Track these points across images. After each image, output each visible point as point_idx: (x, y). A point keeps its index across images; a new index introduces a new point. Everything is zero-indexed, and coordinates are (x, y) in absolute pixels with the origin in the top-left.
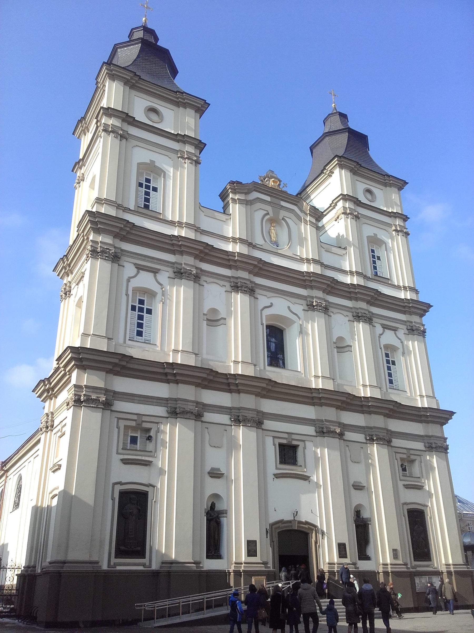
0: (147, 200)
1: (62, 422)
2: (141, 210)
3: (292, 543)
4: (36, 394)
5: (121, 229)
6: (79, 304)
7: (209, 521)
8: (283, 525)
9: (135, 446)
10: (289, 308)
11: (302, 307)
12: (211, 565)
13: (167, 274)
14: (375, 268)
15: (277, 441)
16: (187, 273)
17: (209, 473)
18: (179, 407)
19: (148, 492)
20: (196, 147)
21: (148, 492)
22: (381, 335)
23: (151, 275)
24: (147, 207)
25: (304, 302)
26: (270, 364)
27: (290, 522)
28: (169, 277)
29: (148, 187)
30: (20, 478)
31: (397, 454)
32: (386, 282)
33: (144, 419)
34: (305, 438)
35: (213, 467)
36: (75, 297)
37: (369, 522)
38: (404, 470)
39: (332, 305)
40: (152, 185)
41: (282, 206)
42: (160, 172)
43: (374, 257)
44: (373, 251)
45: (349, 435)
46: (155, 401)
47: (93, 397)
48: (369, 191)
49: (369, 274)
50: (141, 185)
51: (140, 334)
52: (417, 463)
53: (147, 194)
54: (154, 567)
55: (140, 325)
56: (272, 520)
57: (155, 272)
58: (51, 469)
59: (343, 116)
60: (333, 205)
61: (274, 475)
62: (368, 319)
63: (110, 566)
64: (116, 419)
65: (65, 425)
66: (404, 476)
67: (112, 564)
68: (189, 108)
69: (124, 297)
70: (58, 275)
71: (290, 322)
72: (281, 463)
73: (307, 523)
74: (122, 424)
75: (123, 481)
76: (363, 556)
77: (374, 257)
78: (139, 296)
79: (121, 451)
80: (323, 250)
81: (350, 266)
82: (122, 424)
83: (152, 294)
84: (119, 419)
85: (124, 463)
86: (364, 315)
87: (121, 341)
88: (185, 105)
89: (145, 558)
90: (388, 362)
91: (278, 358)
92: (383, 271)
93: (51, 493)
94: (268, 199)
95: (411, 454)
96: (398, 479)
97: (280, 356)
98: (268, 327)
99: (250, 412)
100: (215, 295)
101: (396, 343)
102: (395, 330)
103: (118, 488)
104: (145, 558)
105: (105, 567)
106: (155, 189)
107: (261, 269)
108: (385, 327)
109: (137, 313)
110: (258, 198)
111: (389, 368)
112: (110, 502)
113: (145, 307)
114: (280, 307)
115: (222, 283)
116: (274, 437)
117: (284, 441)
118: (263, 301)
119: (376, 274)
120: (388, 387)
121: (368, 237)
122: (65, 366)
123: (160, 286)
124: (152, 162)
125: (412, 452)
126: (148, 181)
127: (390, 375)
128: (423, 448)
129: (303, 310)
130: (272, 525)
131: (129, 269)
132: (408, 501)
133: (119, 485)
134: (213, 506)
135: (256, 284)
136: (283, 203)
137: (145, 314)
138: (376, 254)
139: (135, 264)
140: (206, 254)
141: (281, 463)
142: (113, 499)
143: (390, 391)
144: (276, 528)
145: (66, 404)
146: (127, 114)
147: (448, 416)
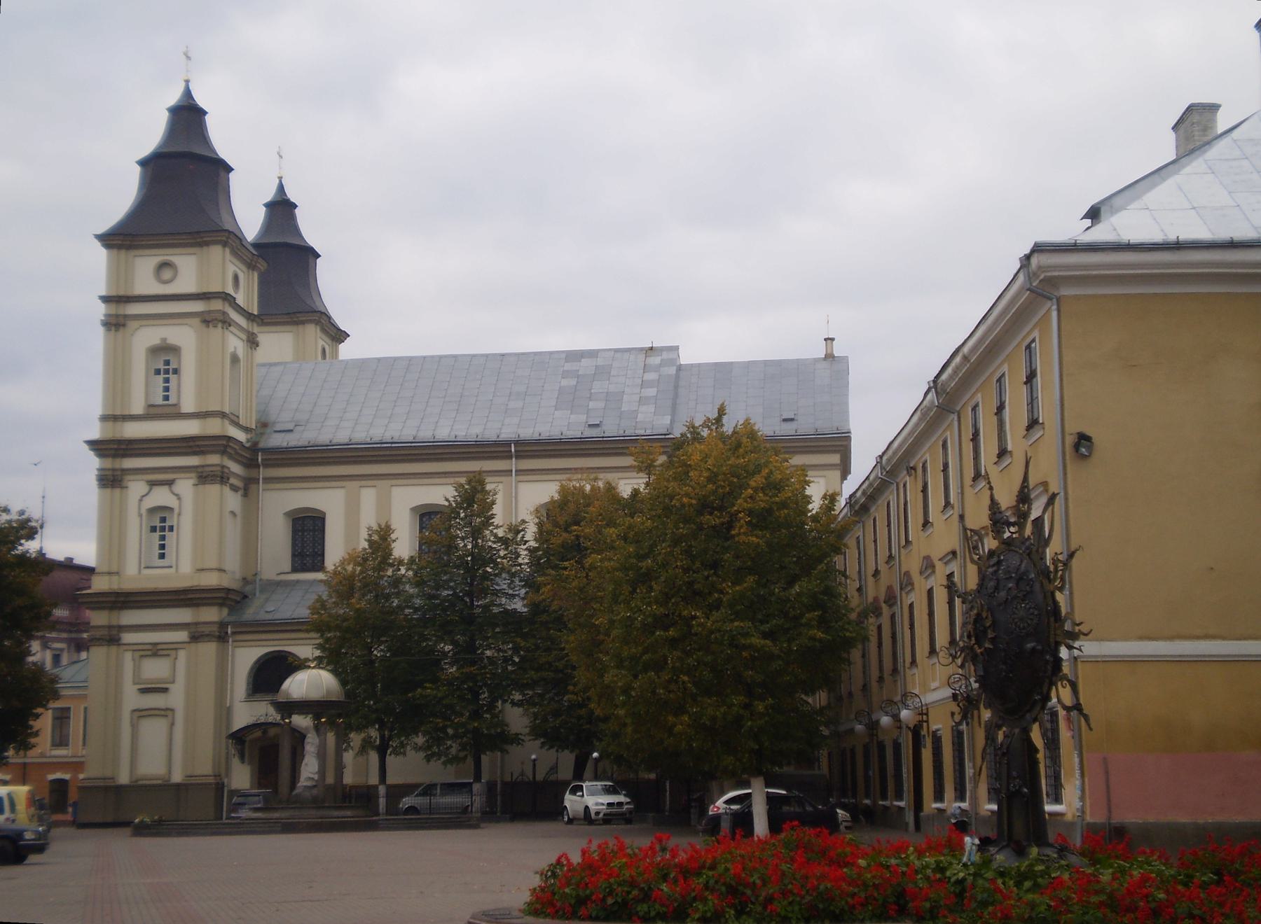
0: (167, 389)
2: (153, 411)
23: (165, 489)
24: (166, 398)
29: (167, 372)
33: (159, 647)
42: (175, 350)
50: (158, 372)
51: (162, 556)
53: (167, 380)
55: (162, 547)
57: (170, 483)
83: (171, 509)
106: (176, 371)
109: (158, 534)
124: (164, 340)
126: (167, 363)
137: (167, 533)
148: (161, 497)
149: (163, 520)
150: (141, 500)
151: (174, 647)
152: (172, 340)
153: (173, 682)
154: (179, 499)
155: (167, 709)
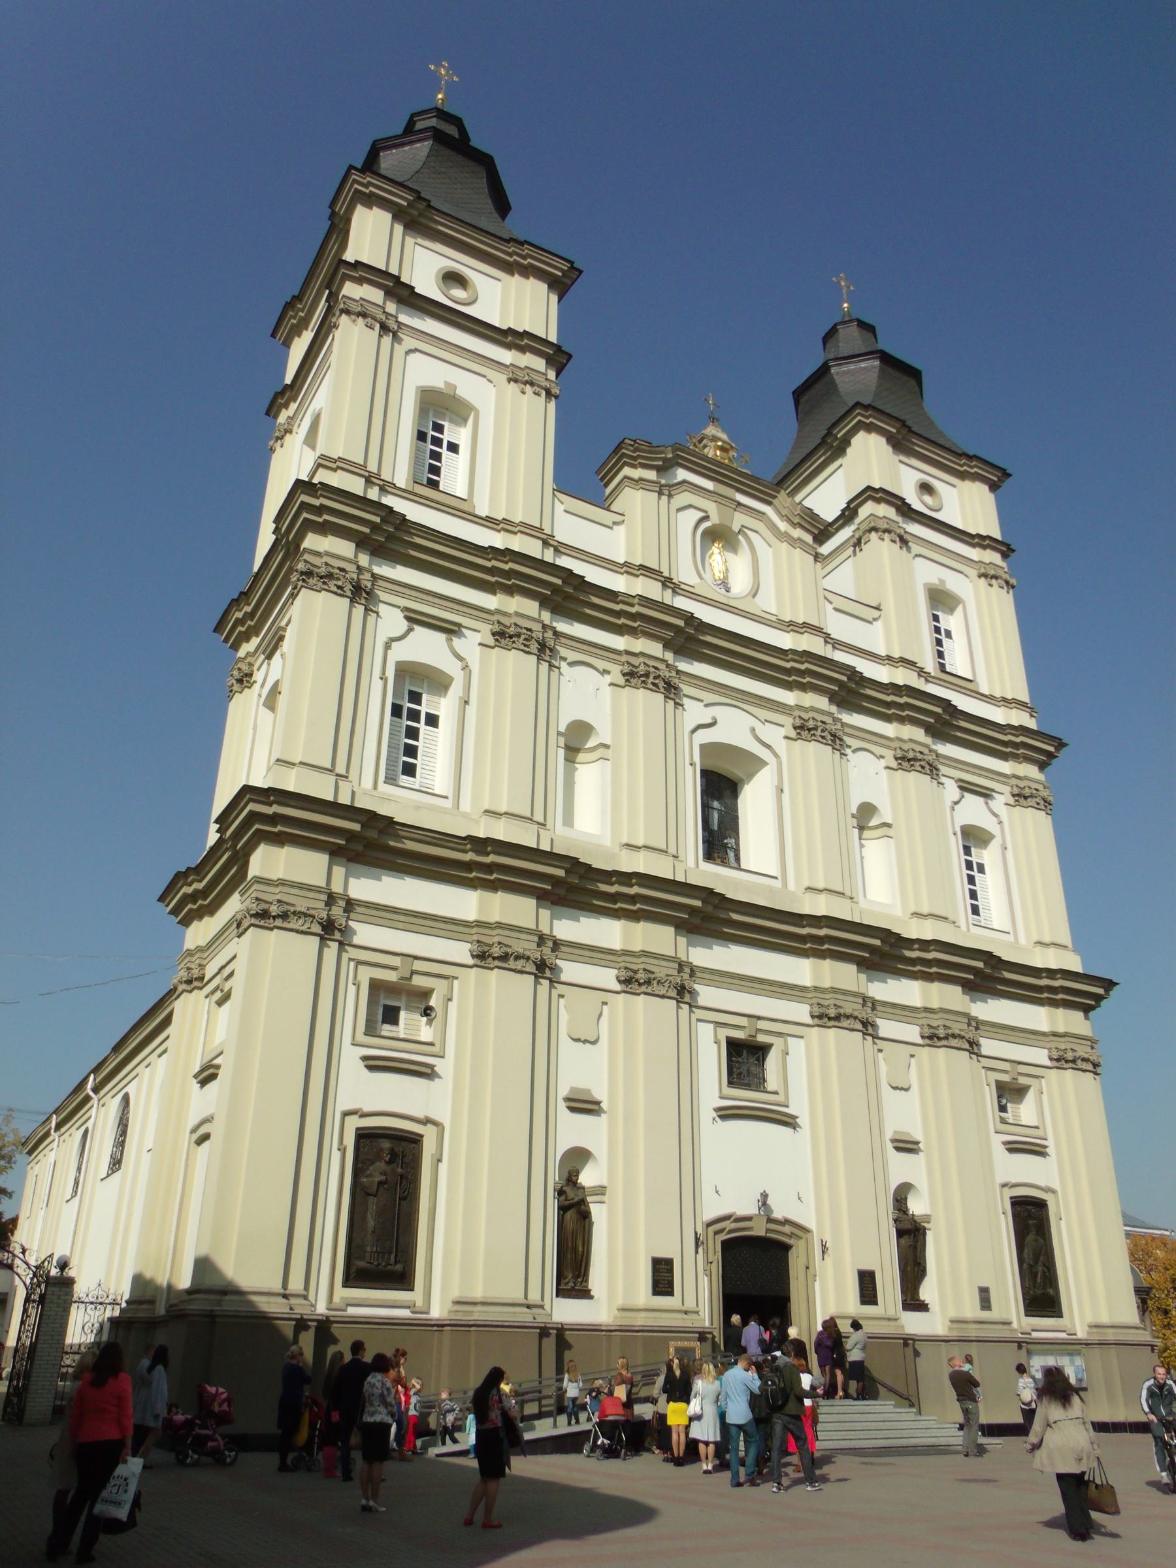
0: (435, 470)
1: (223, 967)
2: (419, 489)
3: (756, 1268)
4: (167, 905)
5: (374, 527)
6: (271, 703)
7: (563, 1209)
8: (734, 1226)
9: (394, 1028)
10: (753, 730)
11: (782, 732)
12: (568, 1312)
13: (477, 638)
14: (941, 655)
15: (724, 1033)
16: (523, 637)
17: (567, 1099)
18: (499, 943)
19: (422, 1136)
20: (550, 361)
21: (422, 1136)
22: (956, 803)
24: (434, 484)
25: (788, 721)
26: (709, 856)
27: (749, 1219)
28: (480, 644)
30: (126, 1099)
31: (989, 1073)
32: (966, 685)
33: (418, 966)
34: (788, 1029)
35: (575, 1085)
36: (262, 686)
37: (926, 1225)
38: (1003, 1109)
39: (847, 730)
40: (446, 437)
41: (739, 504)
43: (937, 630)
44: (936, 618)
45: (886, 1027)
46: (442, 926)
47: (299, 909)
48: (926, 488)
49: (930, 666)
51: (410, 770)
52: (1030, 1096)
53: (436, 456)
54: (437, 1312)
55: (411, 751)
56: (709, 1214)
58: (195, 1076)
59: (867, 327)
60: (848, 514)
61: (718, 1110)
62: (927, 767)
63: (332, 1306)
64: (352, 964)
65: (231, 974)
66: (1003, 1121)
67: (336, 1299)
68: (535, 277)
69: (377, 685)
70: (226, 640)
71: (755, 764)
72: (731, 1083)
73: (787, 1222)
74: (365, 974)
75: (367, 1109)
76: (912, 1303)
77: (937, 630)
78: (411, 684)
79: (361, 1037)
80: (829, 607)
81: (888, 642)
82: (365, 974)
83: (439, 683)
84: (360, 963)
85: (371, 1068)
86: (920, 756)
87: (367, 782)
88: (526, 271)
89: (412, 1290)
90: (969, 865)
91: (725, 846)
92: (958, 663)
93: (194, 1131)
94: (709, 485)
95: (1020, 1074)
96: (992, 1130)
97: (730, 841)
98: (705, 773)
99: (665, 963)
100: (587, 691)
101: (987, 822)
102: (986, 794)
103: (353, 1123)
104: (412, 1290)
105: (321, 1308)
106: (453, 448)
107: (691, 638)
108: (966, 787)
110: (684, 482)
111: (971, 880)
112: (336, 1156)
113: (424, 709)
114: (735, 728)
115: (601, 664)
116: (718, 1024)
117: (740, 1035)
118: (694, 712)
119: (942, 667)
120: (971, 921)
121: (925, 585)
122: (238, 834)
123: (460, 664)
125: (1022, 1069)
127: (973, 895)
128: (1048, 1063)
129: (786, 737)
130: (709, 1225)
131: (390, 620)
132: (1014, 1181)
133: (356, 1117)
134: (571, 1179)
135: (678, 672)
136: (740, 497)
138: (943, 625)
139: (406, 609)
140: (567, 597)
141: (731, 1083)
142: (343, 1150)
143: (974, 930)
144: (716, 1233)
145: (235, 925)
146: (397, 279)
147: (1101, 991)
148: (425, 647)
149: (415, 697)
150: (387, 646)
151: (446, 970)
152: (462, 392)
153: (443, 1057)
154: (465, 668)
155: (427, 1121)
